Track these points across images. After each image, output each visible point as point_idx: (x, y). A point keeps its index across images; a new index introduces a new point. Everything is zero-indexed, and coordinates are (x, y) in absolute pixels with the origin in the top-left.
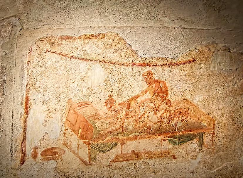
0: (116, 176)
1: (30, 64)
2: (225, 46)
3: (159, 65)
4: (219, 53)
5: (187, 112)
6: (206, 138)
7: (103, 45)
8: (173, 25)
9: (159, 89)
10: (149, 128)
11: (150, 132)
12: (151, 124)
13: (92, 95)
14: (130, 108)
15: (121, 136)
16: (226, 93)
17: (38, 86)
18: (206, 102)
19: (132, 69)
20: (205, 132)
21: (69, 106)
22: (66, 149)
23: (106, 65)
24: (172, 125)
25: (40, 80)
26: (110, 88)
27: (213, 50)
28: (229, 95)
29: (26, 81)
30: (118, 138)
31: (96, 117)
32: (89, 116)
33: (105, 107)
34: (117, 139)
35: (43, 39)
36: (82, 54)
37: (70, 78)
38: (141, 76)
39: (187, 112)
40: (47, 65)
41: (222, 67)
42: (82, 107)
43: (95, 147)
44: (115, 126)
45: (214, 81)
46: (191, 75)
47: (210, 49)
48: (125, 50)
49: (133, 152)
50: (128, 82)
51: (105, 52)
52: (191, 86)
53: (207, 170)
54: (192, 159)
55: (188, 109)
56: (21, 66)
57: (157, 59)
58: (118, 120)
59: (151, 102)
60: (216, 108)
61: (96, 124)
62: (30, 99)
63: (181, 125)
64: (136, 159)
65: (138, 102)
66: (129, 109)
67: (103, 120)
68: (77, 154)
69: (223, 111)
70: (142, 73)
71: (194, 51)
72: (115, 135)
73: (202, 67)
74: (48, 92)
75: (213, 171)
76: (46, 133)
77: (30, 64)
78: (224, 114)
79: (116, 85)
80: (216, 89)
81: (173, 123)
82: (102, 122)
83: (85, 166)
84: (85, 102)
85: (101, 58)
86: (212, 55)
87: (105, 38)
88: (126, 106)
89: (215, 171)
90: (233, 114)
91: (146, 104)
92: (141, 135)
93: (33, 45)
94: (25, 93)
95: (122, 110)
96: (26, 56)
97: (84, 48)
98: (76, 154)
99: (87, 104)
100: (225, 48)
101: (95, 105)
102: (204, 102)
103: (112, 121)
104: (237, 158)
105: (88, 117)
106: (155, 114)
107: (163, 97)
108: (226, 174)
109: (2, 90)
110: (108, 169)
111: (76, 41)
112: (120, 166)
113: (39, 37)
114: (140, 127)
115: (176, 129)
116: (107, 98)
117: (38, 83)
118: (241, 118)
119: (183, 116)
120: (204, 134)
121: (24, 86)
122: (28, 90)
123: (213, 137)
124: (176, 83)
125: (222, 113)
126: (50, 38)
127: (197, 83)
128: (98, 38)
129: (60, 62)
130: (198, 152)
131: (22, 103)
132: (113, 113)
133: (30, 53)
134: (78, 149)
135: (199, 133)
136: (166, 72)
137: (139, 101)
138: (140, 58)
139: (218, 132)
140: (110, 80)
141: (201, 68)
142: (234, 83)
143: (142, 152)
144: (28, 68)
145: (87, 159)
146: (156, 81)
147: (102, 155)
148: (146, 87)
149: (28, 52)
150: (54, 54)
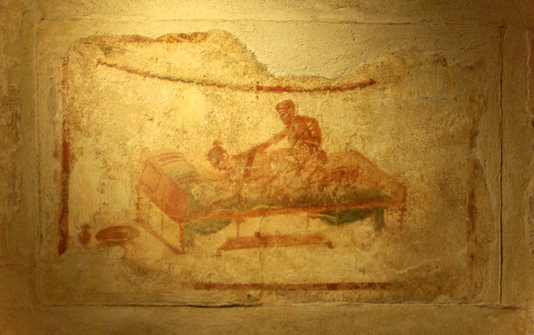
1: (67, 86)
2: (437, 55)
3: (306, 91)
4: (422, 67)
5: (354, 173)
6: (390, 217)
7: (203, 54)
8: (335, 16)
9: (305, 133)
10: (286, 198)
11: (287, 204)
12: (290, 191)
13: (185, 142)
14: (253, 164)
15: (238, 210)
16: (431, 141)
17: (85, 124)
18: (392, 156)
19: (257, 97)
20: (387, 206)
21: (145, 159)
22: (141, 229)
24: (327, 194)
25: (89, 114)
26: (217, 130)
27: (410, 62)
28: (437, 144)
29: (62, 116)
30: (232, 213)
31: (192, 178)
32: (180, 177)
33: (209, 162)
34: (230, 214)
35: (89, 41)
36: (166, 70)
37: (144, 112)
38: (274, 109)
39: (355, 173)
40: (100, 89)
41: (428, 94)
42: (166, 162)
43: (192, 227)
44: (226, 193)
45: (409, 120)
46: (365, 109)
47: (404, 62)
48: (243, 64)
49: (258, 235)
50: (250, 119)
51: (207, 66)
52: (364, 127)
53: (391, 270)
54: (363, 250)
55: (358, 167)
56: (49, 88)
57: (302, 80)
58: (232, 185)
59: (291, 154)
60: (411, 167)
61: (193, 191)
62: (71, 148)
64: (262, 245)
65: (267, 154)
66: (251, 166)
67: (205, 184)
68: (161, 236)
69: (423, 172)
70: (275, 105)
71: (373, 65)
72: (226, 208)
73: (387, 95)
74: (104, 135)
75: (402, 272)
76: (104, 203)
77: (67, 86)
78: (424, 177)
79: (228, 125)
80: (413, 134)
81: (329, 190)
82: (203, 187)
83: (175, 255)
84: (172, 153)
85: (199, 75)
86: (408, 73)
87: (208, 40)
88: (244, 161)
89: (406, 271)
90: (443, 177)
91: (282, 159)
92: (273, 209)
93: (70, 51)
94: (61, 137)
95: (238, 167)
96: (57, 72)
97: (169, 60)
98: (160, 238)
99: (174, 156)
100: (436, 59)
101: (189, 158)
102: (389, 155)
103: (221, 185)
104: (450, 253)
105: (178, 178)
106: (298, 174)
108: (426, 279)
109: (14, 132)
110: (215, 260)
112: (235, 255)
113: (81, 37)
114: (270, 196)
116: (212, 147)
118: (460, 185)
119: (348, 180)
120: (385, 210)
121: (58, 125)
122: (66, 132)
123: (402, 215)
124: (336, 122)
125: (422, 176)
126: (104, 39)
127: (375, 123)
128: (195, 40)
129: (125, 84)
130: (373, 240)
131: (56, 155)
132: (223, 172)
133: (65, 67)
134: (162, 229)
135: (377, 208)
136: (319, 103)
138: (271, 78)
139: (412, 207)
140: (218, 116)
141: (386, 96)
142: (449, 123)
143: (273, 236)
144: (65, 92)
146: (300, 119)
148: (280, 126)
149: (62, 63)
150: (114, 69)
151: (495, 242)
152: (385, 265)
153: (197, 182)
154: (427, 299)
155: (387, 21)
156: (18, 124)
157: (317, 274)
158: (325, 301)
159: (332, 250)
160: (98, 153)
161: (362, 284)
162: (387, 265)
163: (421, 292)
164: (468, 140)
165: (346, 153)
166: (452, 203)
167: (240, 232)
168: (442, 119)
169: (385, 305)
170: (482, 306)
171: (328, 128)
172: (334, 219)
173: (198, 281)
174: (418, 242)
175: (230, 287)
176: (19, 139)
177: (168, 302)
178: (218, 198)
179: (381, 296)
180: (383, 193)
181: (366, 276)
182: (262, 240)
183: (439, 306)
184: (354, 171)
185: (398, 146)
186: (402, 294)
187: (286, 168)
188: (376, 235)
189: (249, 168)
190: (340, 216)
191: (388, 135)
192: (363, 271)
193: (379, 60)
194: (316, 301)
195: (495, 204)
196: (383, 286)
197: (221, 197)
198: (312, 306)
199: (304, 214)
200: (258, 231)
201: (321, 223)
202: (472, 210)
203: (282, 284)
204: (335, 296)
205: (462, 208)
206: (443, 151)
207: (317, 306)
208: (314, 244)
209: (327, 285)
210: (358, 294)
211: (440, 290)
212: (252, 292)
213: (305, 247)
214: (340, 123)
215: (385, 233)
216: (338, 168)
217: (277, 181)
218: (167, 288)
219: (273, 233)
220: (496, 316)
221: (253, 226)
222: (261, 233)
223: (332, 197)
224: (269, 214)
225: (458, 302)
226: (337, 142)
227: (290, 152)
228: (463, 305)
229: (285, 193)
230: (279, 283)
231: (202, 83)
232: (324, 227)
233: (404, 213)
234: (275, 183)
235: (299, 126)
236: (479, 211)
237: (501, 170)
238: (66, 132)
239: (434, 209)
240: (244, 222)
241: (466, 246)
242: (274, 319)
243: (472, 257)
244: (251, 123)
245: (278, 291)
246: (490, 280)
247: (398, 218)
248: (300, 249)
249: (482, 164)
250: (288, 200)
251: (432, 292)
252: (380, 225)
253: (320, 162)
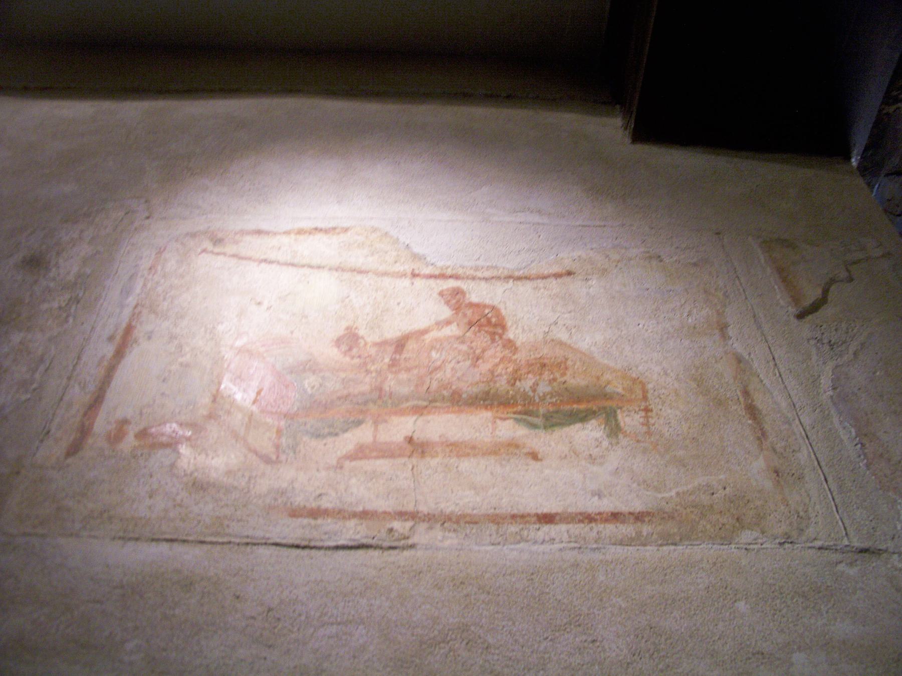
0: (355, 490)
5: (561, 365)
6: (627, 419)
11: (458, 402)
14: (405, 351)
19: (413, 284)
23: (346, 275)
24: (522, 390)
27: (616, 257)
33: (336, 350)
38: (435, 295)
39: (563, 366)
47: (607, 256)
49: (410, 440)
50: (401, 304)
55: (567, 359)
59: (463, 342)
62: (136, 331)
63: (548, 389)
70: (437, 290)
72: (358, 403)
75: (667, 495)
82: (323, 378)
88: (390, 349)
89: (673, 493)
90: (697, 371)
92: (436, 407)
106: (474, 365)
107: (494, 333)
108: (712, 506)
111: (278, 237)
115: (537, 398)
117: (166, 304)
118: (723, 381)
120: (619, 411)
123: (647, 417)
130: (607, 449)
131: (111, 338)
135: (604, 408)
137: (427, 341)
139: (660, 407)
142: (685, 314)
146: (471, 305)
147: (314, 443)
148: (446, 312)
151: (805, 452)
152: (635, 485)
153: (314, 372)
154: (722, 538)
155: (578, 223)
156: (73, 308)
157: (517, 499)
158: (535, 542)
159: (539, 463)
160: (172, 337)
161: (600, 514)
162: (639, 485)
163: (708, 526)
164: (717, 331)
165: (545, 342)
167: (378, 436)
168: (673, 310)
169: (648, 548)
170: (820, 548)
171: (515, 315)
172: (538, 421)
173: (297, 503)
174: (681, 453)
175: (354, 515)
176: (67, 322)
177: (236, 536)
178: (345, 392)
179: (639, 534)
180: (609, 389)
181: (605, 501)
182: (416, 447)
183: (746, 549)
184: (561, 362)
185: (620, 336)
186: (676, 530)
187: (455, 358)
188: (611, 443)
189: (398, 357)
190: (547, 417)
191: (604, 325)
192: (599, 494)
193: (576, 254)
194: (519, 542)
195: (784, 404)
196: (639, 517)
197: (351, 390)
198: (512, 550)
199: (488, 414)
200: (410, 434)
201: (517, 426)
202: (752, 411)
203: (452, 513)
204: (553, 534)
205: (738, 409)
206: (686, 343)
207: (522, 551)
208: (508, 454)
209: (537, 515)
210: (595, 530)
212: (396, 525)
213: (492, 459)
214: (531, 315)
215: (624, 442)
216: (536, 359)
217: (442, 373)
218: (239, 513)
219: (435, 438)
220: (851, 564)
221: (401, 427)
222: (415, 438)
223: (531, 394)
224: (429, 413)
225: (777, 541)
226: (531, 331)
227: (461, 339)
228: (787, 545)
229: (454, 387)
230: (448, 511)
231: (339, 269)
232: (521, 432)
233: (650, 414)
234: (439, 375)
235: (473, 313)
236: (764, 412)
237: (776, 365)
238: (136, 315)
239: (695, 410)
240: (386, 421)
241: (761, 457)
242: (439, 572)
243: (776, 472)
244: (404, 308)
245: (446, 525)
246: (818, 507)
247: (642, 420)
248: (483, 462)
249: (747, 357)
250: (460, 396)
251: (727, 526)
253: (507, 351)
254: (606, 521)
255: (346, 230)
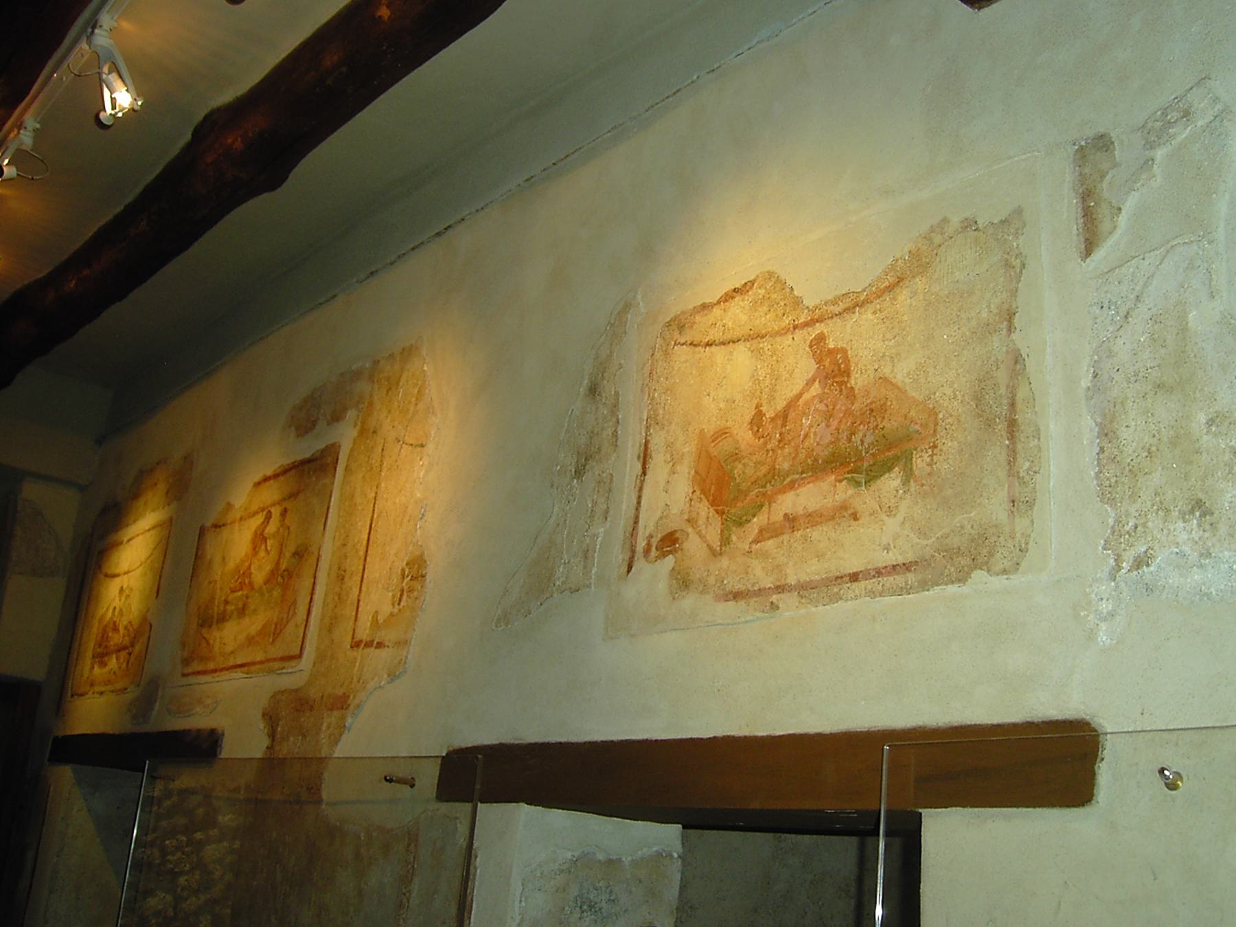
22: (690, 530)
67: (746, 461)
88: (779, 422)
145: (716, 545)
166: (989, 424)
172: (862, 478)
205: (1001, 427)
211: (975, 564)
252: (908, 475)
254: (889, 574)
255: (752, 282)
